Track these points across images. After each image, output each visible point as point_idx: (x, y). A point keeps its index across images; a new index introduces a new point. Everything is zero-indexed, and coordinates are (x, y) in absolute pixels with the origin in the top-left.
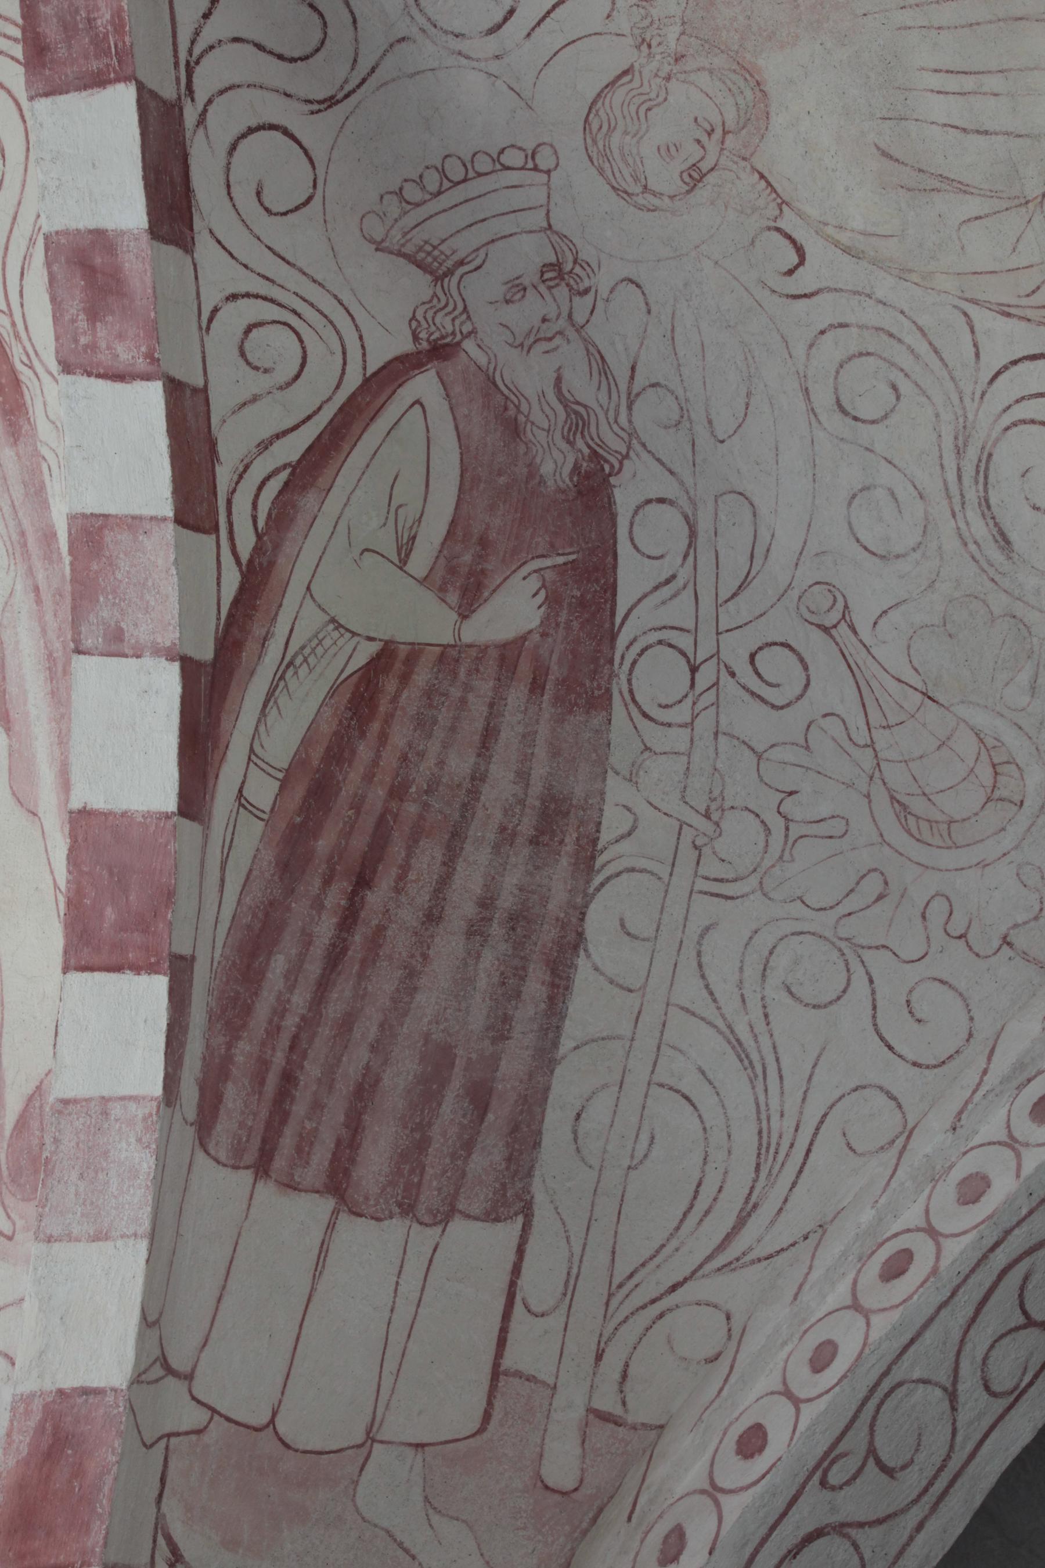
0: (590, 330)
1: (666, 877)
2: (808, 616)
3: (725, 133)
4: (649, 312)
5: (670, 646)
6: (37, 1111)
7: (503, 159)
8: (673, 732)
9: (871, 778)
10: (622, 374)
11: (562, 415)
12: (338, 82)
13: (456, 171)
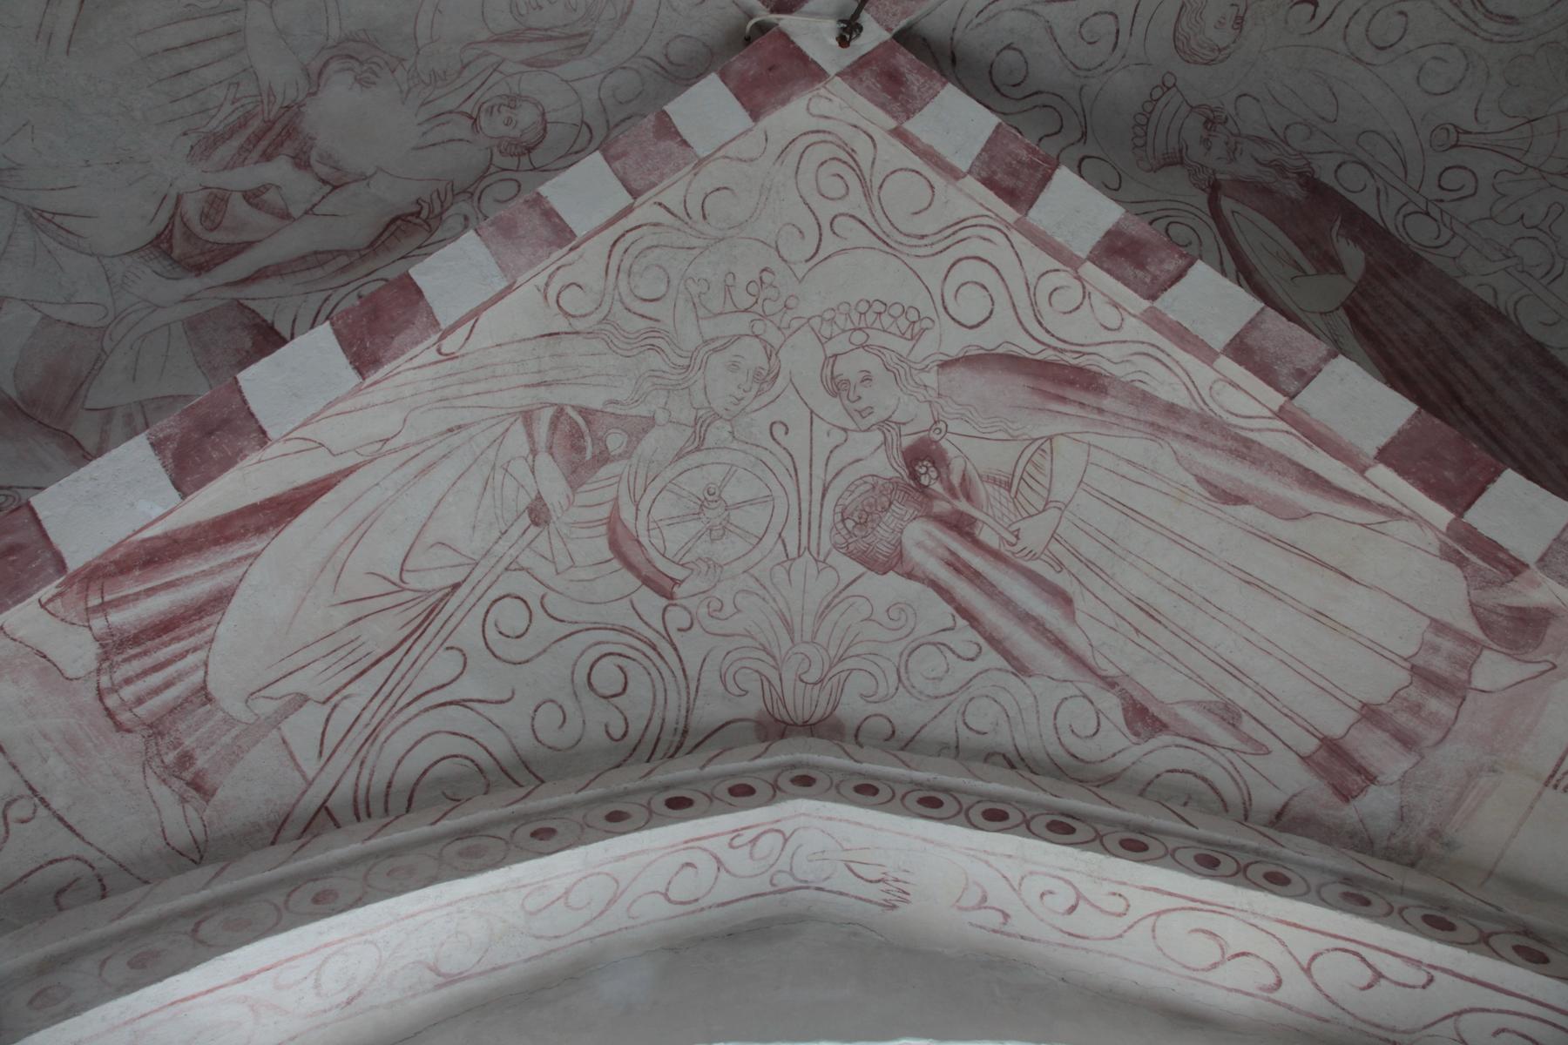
2: (1442, 149)
4: (1258, 101)
5: (1409, 214)
6: (1486, 612)
10: (1271, 136)
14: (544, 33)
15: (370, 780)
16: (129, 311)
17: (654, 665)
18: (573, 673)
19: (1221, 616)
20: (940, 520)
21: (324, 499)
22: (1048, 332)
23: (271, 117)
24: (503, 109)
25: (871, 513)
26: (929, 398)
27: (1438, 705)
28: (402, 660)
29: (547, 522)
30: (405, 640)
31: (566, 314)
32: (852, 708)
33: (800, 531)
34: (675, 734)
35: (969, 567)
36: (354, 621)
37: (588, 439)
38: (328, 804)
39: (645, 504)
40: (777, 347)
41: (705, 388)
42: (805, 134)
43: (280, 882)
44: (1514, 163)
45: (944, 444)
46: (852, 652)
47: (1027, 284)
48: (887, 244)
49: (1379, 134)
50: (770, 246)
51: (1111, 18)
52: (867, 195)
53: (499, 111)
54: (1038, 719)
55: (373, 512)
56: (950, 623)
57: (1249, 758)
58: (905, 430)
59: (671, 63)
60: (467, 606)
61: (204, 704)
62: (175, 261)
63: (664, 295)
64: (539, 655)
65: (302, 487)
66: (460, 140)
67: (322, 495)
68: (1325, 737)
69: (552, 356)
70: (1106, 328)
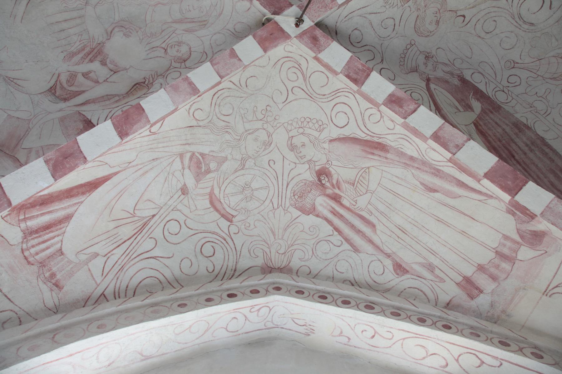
0: (439, 61)
1: (539, 119)
3: (439, 10)
4: (444, 50)
5: (497, 91)
6: (522, 232)
7: (408, 48)
8: (512, 101)
9: (544, 79)
11: (448, 75)
12: (380, 57)
13: (403, 56)
14: (192, 20)
15: (120, 285)
16: (39, 114)
17: (225, 246)
18: (195, 248)
19: (428, 232)
20: (329, 196)
21: (107, 183)
22: (368, 130)
23: (94, 47)
24: (176, 46)
25: (304, 193)
26: (325, 153)
27: (505, 266)
28: (133, 242)
29: (187, 194)
30: (135, 234)
31: (196, 120)
32: (295, 263)
33: (278, 199)
34: (231, 271)
35: (339, 213)
36: (116, 227)
37: (203, 164)
38: (104, 293)
39: (223, 188)
40: (271, 133)
41: (246, 147)
42: (283, 58)
43: (86, 320)
44: (534, 74)
45: (331, 169)
46: (296, 243)
47: (361, 113)
48: (312, 98)
49: (486, 63)
50: (270, 97)
51: (393, 20)
52: (305, 80)
53: (174, 47)
54: (362, 268)
55: (125, 188)
56: (331, 233)
57: (437, 283)
58: (317, 164)
59: (236, 32)
60: (158, 223)
61: (60, 256)
62: (58, 97)
63: (232, 114)
64: (183, 241)
65: (99, 178)
66: (160, 57)
67: (106, 182)
68: (465, 276)
69: (191, 134)
70: (389, 129)
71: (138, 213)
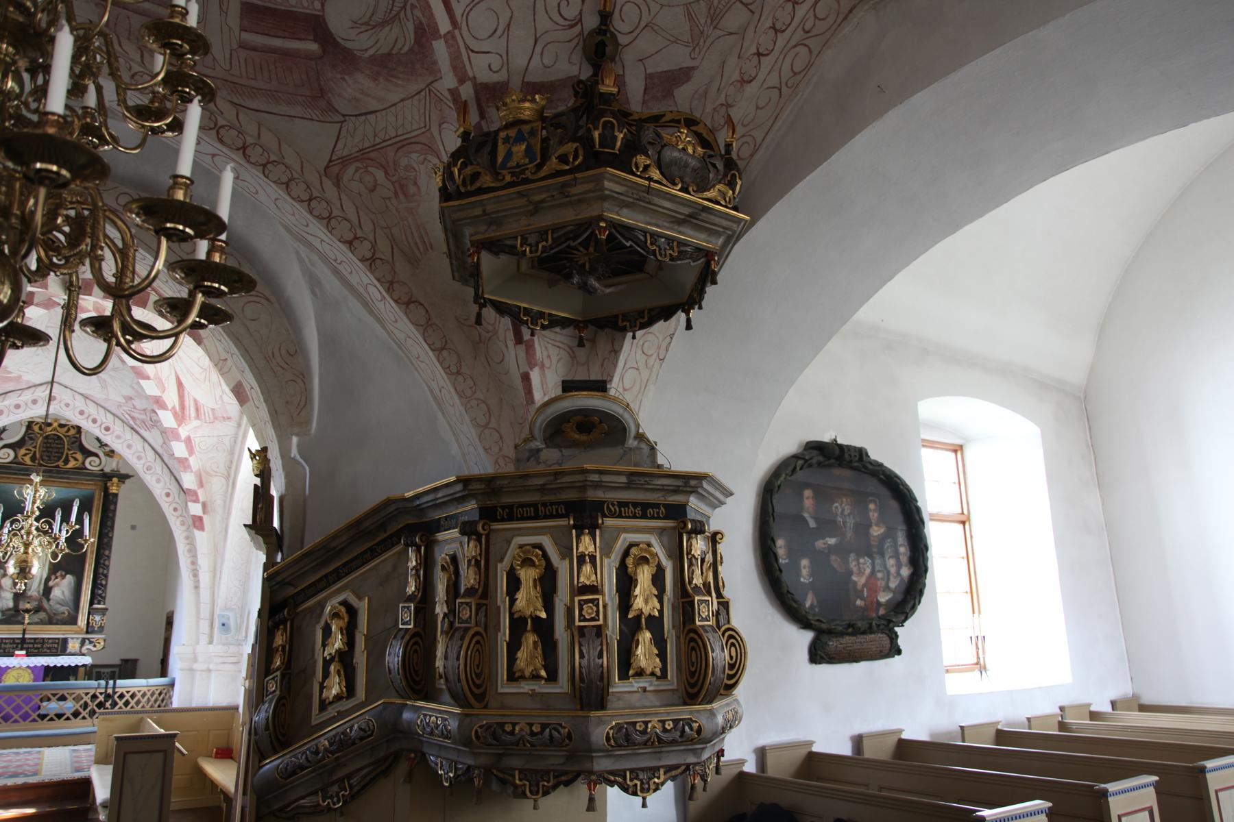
71: (205, 367)
